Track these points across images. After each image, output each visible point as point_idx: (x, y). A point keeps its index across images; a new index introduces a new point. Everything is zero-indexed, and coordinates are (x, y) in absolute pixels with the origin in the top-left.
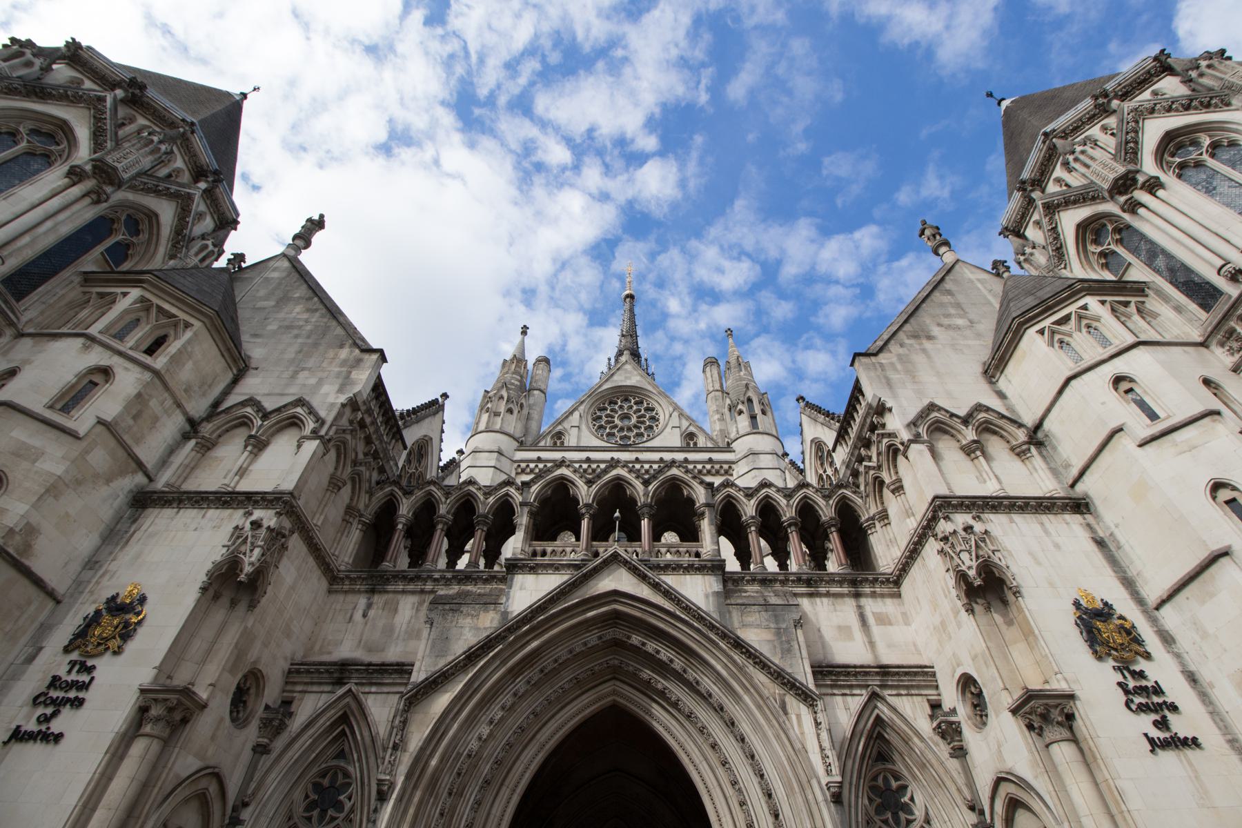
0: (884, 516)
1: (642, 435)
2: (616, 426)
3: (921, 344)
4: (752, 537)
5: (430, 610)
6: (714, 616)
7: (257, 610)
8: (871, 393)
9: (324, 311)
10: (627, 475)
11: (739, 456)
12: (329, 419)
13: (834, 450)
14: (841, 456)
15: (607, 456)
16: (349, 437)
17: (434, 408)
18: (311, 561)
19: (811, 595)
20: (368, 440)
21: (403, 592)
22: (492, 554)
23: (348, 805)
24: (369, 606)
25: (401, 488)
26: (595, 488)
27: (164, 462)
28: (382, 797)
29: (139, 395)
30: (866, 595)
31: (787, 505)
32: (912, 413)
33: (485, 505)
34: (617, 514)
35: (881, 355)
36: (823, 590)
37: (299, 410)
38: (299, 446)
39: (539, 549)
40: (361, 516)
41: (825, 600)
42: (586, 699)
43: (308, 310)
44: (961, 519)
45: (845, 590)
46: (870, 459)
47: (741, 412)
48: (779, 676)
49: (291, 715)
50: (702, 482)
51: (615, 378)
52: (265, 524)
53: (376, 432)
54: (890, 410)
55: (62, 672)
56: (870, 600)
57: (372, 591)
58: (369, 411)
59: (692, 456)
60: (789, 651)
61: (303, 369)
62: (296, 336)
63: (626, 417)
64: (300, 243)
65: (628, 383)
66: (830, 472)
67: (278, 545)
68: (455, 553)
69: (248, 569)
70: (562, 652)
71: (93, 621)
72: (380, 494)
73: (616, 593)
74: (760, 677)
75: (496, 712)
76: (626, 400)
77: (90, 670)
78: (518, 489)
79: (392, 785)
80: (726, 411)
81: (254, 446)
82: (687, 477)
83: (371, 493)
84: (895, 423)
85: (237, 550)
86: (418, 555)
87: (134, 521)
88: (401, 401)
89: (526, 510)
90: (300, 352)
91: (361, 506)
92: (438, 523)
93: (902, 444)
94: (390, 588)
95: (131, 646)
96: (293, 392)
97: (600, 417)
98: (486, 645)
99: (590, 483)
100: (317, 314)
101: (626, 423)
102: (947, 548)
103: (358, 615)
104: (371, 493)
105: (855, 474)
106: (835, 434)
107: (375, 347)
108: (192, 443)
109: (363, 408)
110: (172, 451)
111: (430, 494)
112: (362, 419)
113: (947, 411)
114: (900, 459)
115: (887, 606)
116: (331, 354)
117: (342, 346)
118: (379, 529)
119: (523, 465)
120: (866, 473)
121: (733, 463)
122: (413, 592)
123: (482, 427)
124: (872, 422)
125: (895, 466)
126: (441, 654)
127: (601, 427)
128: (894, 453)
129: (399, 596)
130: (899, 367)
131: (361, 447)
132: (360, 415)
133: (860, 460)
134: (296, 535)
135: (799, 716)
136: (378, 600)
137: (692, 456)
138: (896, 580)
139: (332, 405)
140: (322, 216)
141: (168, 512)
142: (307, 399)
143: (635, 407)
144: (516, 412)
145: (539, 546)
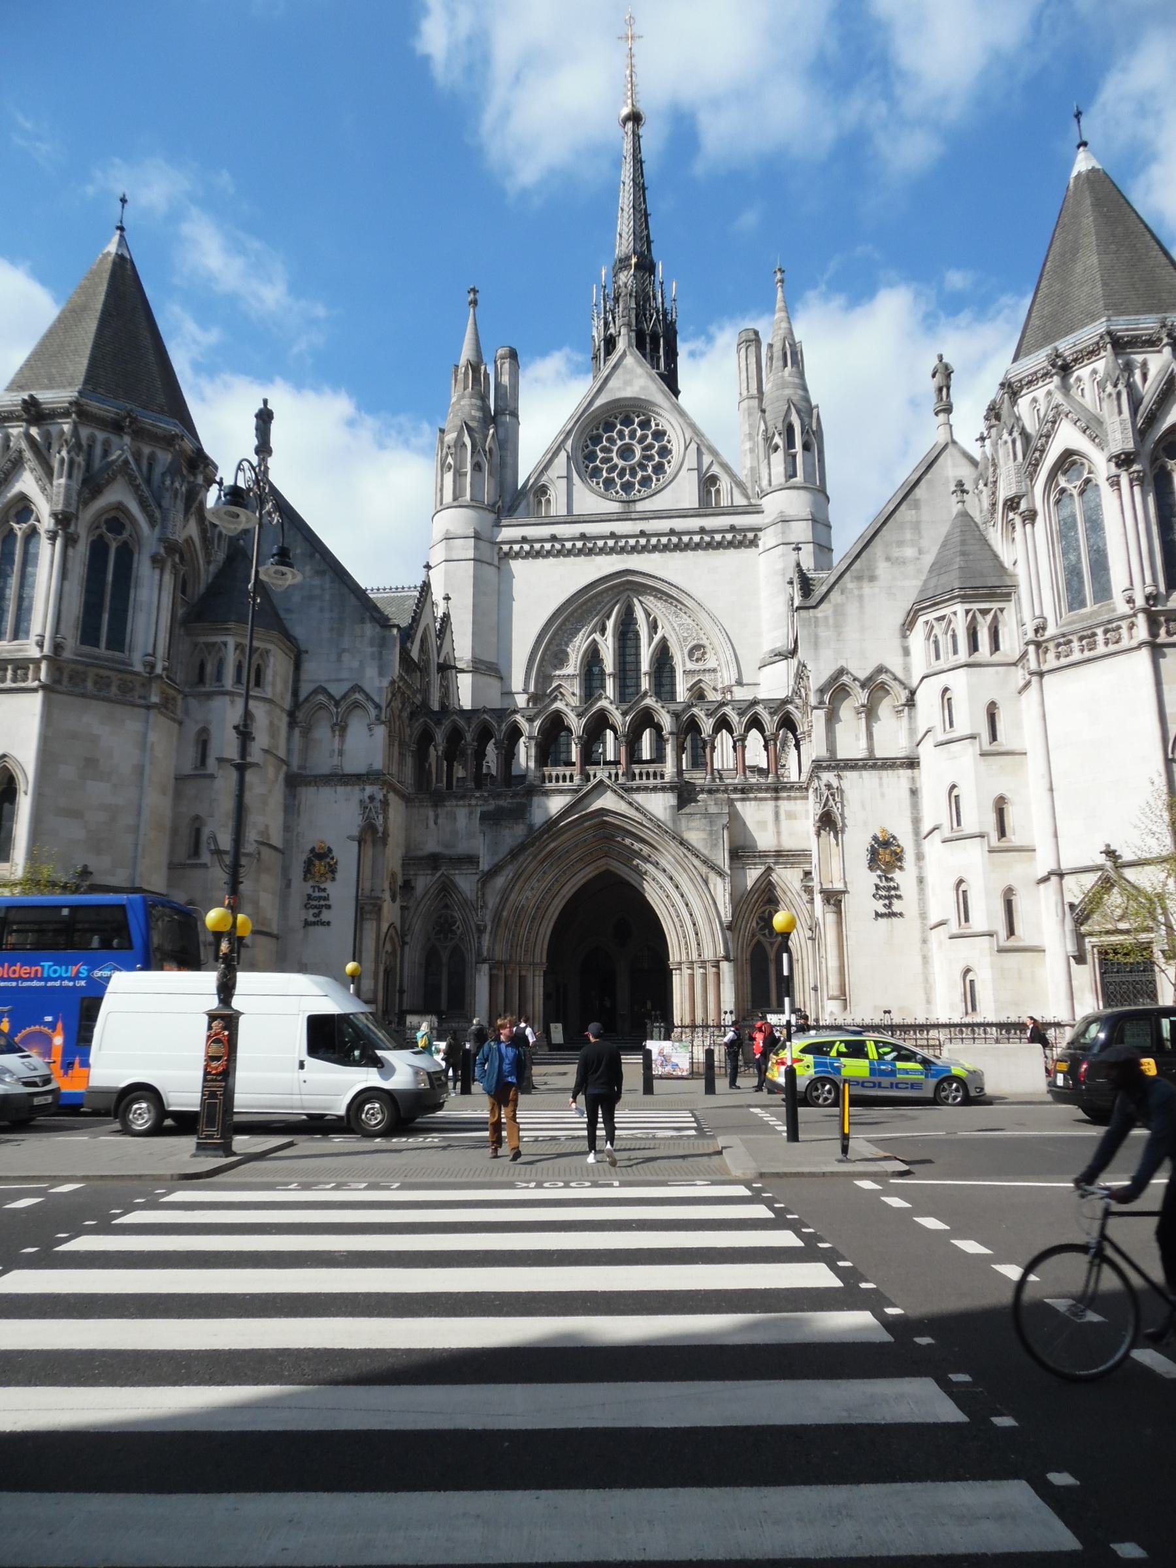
2: (616, 466)
3: (861, 588)
5: (481, 824)
6: (670, 824)
11: (768, 520)
12: (384, 705)
19: (743, 800)
23: (459, 932)
24: (437, 817)
26: (584, 720)
27: (289, 751)
28: (481, 931)
29: (271, 724)
30: (784, 799)
31: (740, 723)
36: (751, 795)
37: (358, 696)
42: (588, 869)
44: (828, 777)
45: (769, 795)
47: (776, 448)
49: (413, 888)
51: (611, 384)
55: (310, 891)
56: (785, 802)
57: (436, 806)
59: (710, 523)
60: (716, 845)
61: (344, 650)
62: (321, 610)
65: (628, 393)
69: (381, 829)
71: (309, 864)
74: (697, 862)
77: (324, 890)
79: (485, 926)
80: (760, 437)
85: (368, 817)
87: (295, 797)
91: (407, 739)
95: (338, 876)
103: (431, 823)
108: (297, 731)
110: (289, 740)
111: (454, 721)
115: (797, 806)
117: (362, 621)
121: (760, 530)
122: (464, 806)
130: (831, 621)
135: (715, 885)
136: (439, 810)
137: (710, 523)
138: (807, 789)
139: (380, 689)
141: (312, 790)
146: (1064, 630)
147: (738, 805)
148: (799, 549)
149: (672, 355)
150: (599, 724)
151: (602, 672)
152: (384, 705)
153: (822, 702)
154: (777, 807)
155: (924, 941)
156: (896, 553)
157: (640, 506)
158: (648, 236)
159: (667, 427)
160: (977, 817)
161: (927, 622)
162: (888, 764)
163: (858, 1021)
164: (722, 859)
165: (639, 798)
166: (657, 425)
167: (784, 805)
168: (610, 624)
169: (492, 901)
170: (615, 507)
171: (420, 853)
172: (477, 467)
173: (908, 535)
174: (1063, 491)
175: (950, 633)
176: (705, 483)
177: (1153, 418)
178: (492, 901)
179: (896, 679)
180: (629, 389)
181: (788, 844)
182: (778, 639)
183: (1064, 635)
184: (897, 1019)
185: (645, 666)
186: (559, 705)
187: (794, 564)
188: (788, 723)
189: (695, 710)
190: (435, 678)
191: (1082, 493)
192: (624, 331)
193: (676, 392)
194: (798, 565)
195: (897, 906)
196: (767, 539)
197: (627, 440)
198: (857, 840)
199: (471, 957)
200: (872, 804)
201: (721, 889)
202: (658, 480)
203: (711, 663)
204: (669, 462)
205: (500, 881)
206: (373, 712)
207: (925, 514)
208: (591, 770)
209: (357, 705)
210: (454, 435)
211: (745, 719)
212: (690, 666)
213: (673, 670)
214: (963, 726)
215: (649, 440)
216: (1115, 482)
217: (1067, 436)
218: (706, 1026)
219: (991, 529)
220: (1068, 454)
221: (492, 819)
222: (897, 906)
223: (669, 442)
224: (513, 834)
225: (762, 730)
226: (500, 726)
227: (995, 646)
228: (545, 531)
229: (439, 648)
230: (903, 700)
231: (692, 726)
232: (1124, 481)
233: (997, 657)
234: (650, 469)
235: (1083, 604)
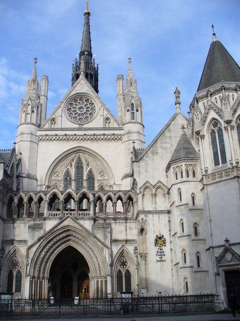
3: (153, 155)
6: (91, 231)
11: (126, 132)
26: (63, 195)
28: (27, 266)
33: (35, 199)
44: (142, 216)
45: (124, 221)
47: (128, 111)
48: (103, 243)
60: (106, 238)
63: (81, 108)
70: (58, 238)
75: (45, 250)
80: (123, 107)
83: (6, 196)
84: (139, 186)
91: (5, 201)
98: (42, 238)
99: (62, 194)
119: (41, 138)
126: (33, 239)
146: (213, 172)
147: (113, 226)
148: (134, 143)
149: (97, 80)
150: (69, 197)
151: (70, 178)
153: (140, 192)
155: (172, 269)
156: (164, 145)
157: (85, 126)
158: (91, 46)
159: (94, 102)
160: (188, 229)
161: (173, 168)
162: (161, 212)
163: (151, 296)
164: (108, 243)
165: (81, 222)
167: (128, 224)
168: (73, 164)
169: (31, 255)
170: (77, 126)
171: (7, 239)
172: (33, 111)
173: (168, 140)
174: (213, 130)
175: (180, 171)
177: (235, 111)
178: (31, 255)
179: (164, 185)
181: (130, 238)
182: (128, 171)
183: (213, 173)
184: (163, 295)
185: (85, 178)
186: (55, 190)
187: (132, 147)
188: (130, 199)
189: (100, 193)
190: (15, 179)
191: (218, 132)
192: (82, 73)
193: (97, 92)
194: (134, 148)
195: (164, 258)
196: (125, 138)
198: (151, 237)
199: (24, 274)
200: (156, 226)
201: (106, 252)
202: (91, 118)
203: (106, 178)
205: (34, 249)
207: (172, 134)
208: (66, 212)
210: (26, 102)
211: (116, 197)
212: (99, 178)
213: (93, 179)
214: (184, 202)
216: (226, 129)
217: (213, 114)
218: (102, 299)
219: (192, 140)
220: (214, 119)
221: (33, 228)
222: (163, 259)
224: (41, 233)
225: (122, 201)
227: (194, 176)
229: (17, 170)
230: (166, 192)
231: (99, 198)
232: (229, 128)
233: (194, 179)
235: (219, 164)
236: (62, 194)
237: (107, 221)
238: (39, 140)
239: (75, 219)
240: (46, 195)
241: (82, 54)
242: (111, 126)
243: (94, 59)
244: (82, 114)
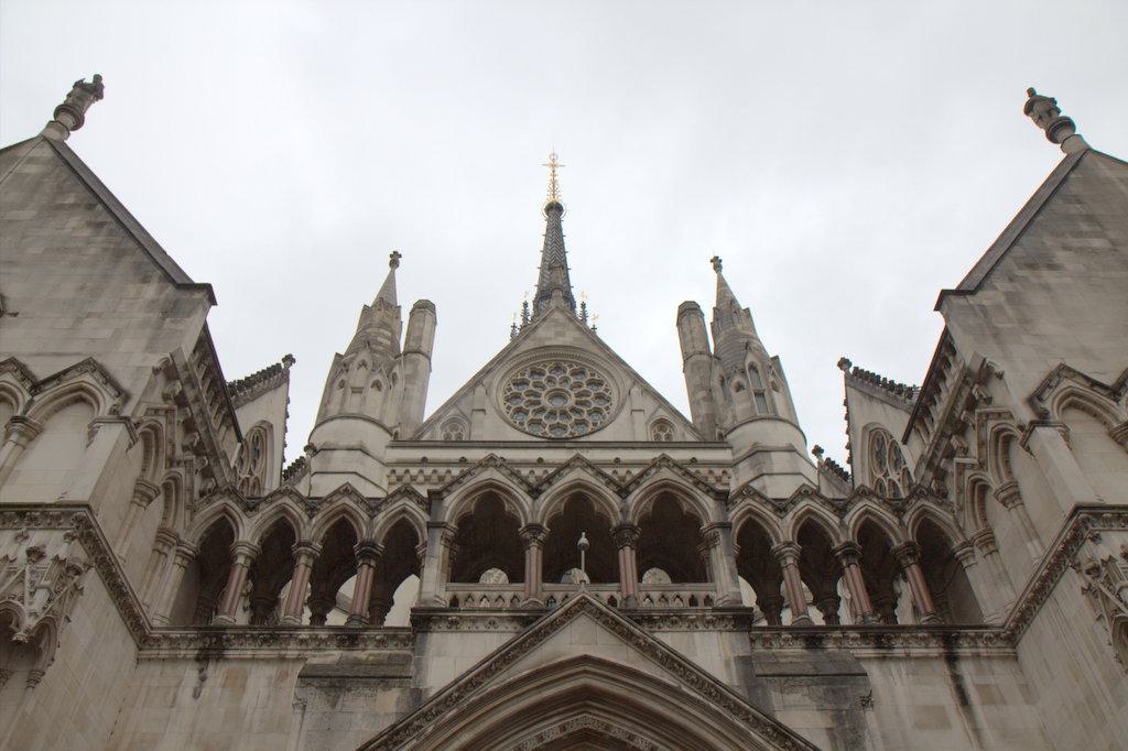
0: (988, 540)
1: (582, 423)
2: (543, 410)
4: (791, 573)
6: (740, 692)
7: (40, 687)
8: (968, 353)
9: (114, 226)
10: (593, 480)
13: (905, 441)
14: (913, 453)
15: (533, 455)
16: (162, 420)
17: (276, 376)
18: (113, 611)
20: (189, 427)
21: (254, 660)
22: (381, 602)
25: (239, 501)
31: (842, 524)
32: (1031, 385)
33: (373, 529)
34: (583, 540)
35: (980, 294)
36: (899, 652)
37: (88, 379)
38: (92, 434)
39: (461, 595)
40: (180, 543)
41: (903, 666)
43: (89, 224)
46: (966, 451)
47: (739, 387)
50: (709, 490)
51: (541, 333)
52: (50, 553)
53: (204, 406)
54: (1000, 376)
57: (203, 658)
58: (190, 381)
61: (89, 315)
63: (558, 395)
64: (68, 120)
65: (560, 341)
66: (894, 476)
67: (70, 583)
68: (323, 600)
69: (30, 622)
72: (207, 512)
73: (586, 659)
76: (558, 368)
78: (420, 501)
80: (715, 382)
81: (22, 434)
82: (687, 483)
83: (193, 510)
86: (263, 603)
88: (234, 369)
89: (438, 533)
90: (82, 288)
91: (179, 528)
92: (299, 555)
93: (1021, 428)
94: (230, 654)
96: (77, 351)
97: (516, 396)
99: (535, 492)
100: (105, 230)
101: (558, 404)
102: (1099, 584)
103: (186, 695)
104: (193, 510)
105: (941, 475)
106: (906, 418)
107: (197, 280)
109: (184, 376)
112: (182, 392)
113: (1087, 378)
114: (1017, 450)
116: (132, 290)
117: (146, 280)
118: (208, 564)
119: (400, 471)
120: (960, 473)
122: (267, 661)
123: (334, 409)
124: (971, 396)
125: (1007, 462)
127: (519, 410)
128: (1004, 440)
129: (248, 666)
131: (179, 438)
132: (178, 387)
133: (950, 454)
134: (92, 572)
136: (216, 673)
138: (1011, 636)
140: (98, 78)
142: (99, 360)
143: (573, 380)
144: (384, 387)
145: (462, 590)
147: (874, 672)
152: (137, 392)
154: (957, 679)
166: (592, 375)
173: (1084, 227)
176: (652, 426)
180: (561, 339)
197: (558, 386)
204: (607, 408)
206: (107, 401)
209: (81, 397)
211: (852, 517)
215: (585, 387)
223: (607, 390)
226: (372, 518)
228: (455, 455)
234: (585, 416)
236: (535, 492)
237: (831, 646)
238: (393, 478)
239: (630, 623)
240: (433, 500)
241: (543, 295)
242: (677, 437)
243: (583, 306)
244: (564, 413)
